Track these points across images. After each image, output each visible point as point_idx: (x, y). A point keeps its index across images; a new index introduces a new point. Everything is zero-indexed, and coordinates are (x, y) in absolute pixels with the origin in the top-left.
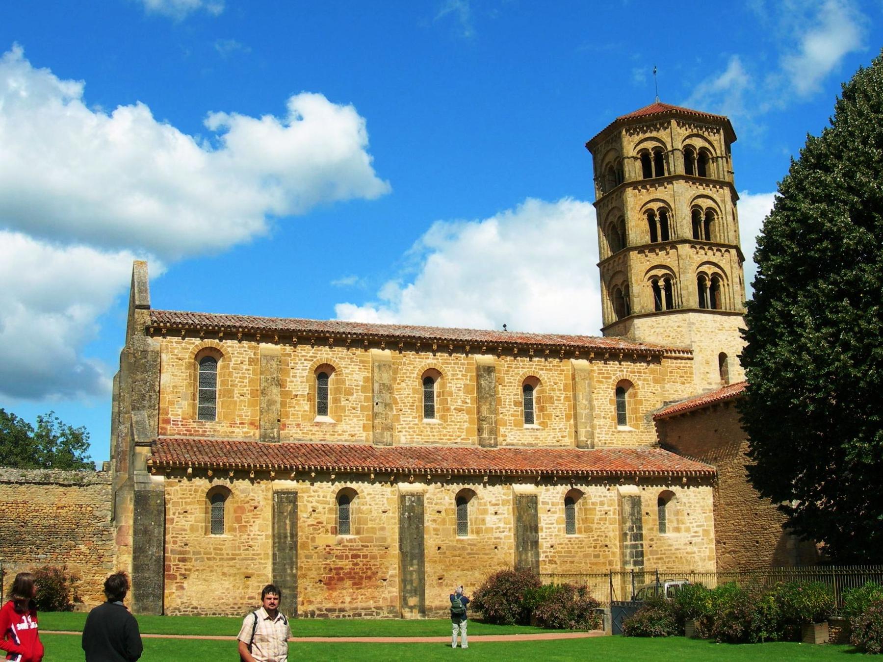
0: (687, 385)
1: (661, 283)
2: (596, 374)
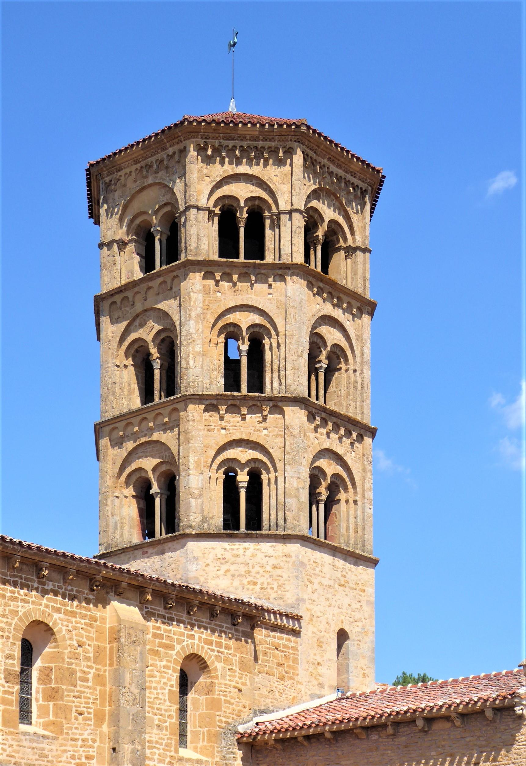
0: (288, 682)
1: (243, 477)
2: (149, 636)
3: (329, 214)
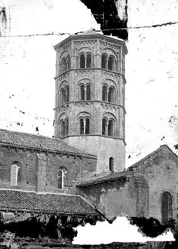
3: (109, 53)
